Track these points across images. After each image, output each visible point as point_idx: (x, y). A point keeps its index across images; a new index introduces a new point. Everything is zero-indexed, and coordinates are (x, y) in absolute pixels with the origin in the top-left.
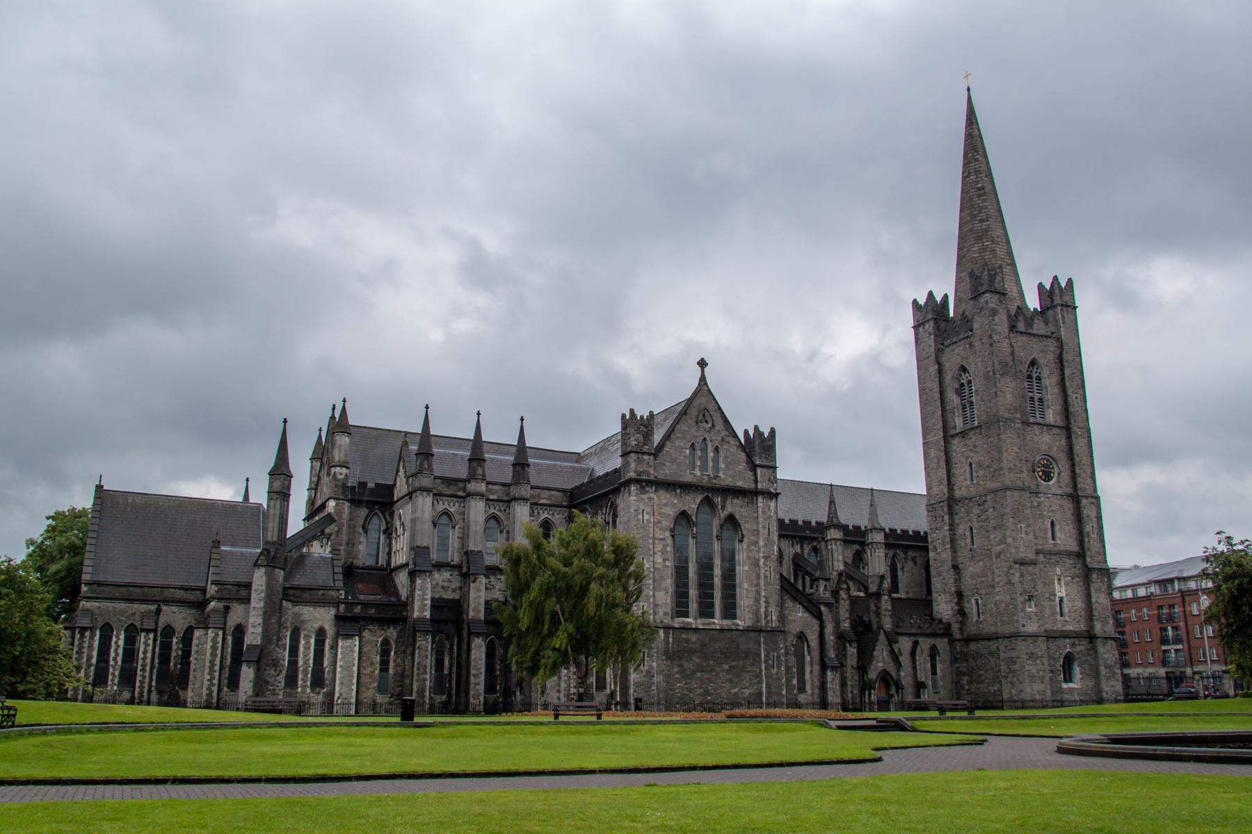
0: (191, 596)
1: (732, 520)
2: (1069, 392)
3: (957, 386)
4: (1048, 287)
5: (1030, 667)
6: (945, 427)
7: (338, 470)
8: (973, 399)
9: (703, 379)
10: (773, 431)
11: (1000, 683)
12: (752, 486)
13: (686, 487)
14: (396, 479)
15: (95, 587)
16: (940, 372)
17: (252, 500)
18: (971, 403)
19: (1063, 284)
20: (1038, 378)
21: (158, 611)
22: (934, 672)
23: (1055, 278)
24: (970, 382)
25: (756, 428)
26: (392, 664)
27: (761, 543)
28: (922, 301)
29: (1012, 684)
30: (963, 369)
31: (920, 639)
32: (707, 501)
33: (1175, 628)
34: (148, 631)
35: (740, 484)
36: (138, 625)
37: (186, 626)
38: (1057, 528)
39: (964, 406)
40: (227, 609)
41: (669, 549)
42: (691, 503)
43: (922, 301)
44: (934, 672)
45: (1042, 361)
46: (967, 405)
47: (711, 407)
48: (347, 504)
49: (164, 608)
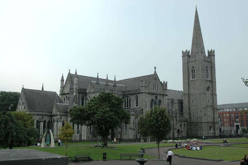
0: (49, 114)
1: (160, 100)
2: (213, 73)
3: (191, 70)
4: (210, 51)
5: (205, 129)
6: (188, 80)
7: (76, 86)
8: (195, 74)
9: (155, 71)
10: (167, 82)
11: (198, 131)
12: (163, 94)
13: (153, 94)
14: (87, 88)
15: (30, 112)
16: (188, 67)
17: (44, 90)
18: (194, 75)
19: (213, 50)
20: (208, 70)
21: (43, 117)
22: (184, 129)
23: (212, 50)
24: (194, 70)
25: (164, 81)
26: (92, 128)
27: (165, 105)
28: (184, 51)
29: (201, 131)
30: (193, 67)
31: (182, 122)
32: (156, 96)
33: (220, 119)
34: (42, 122)
35: (161, 93)
36: (39, 120)
37: (48, 120)
38: (209, 100)
39: (193, 75)
40: (61, 117)
41: (150, 106)
42: (154, 97)
43: (184, 51)
44: (184, 129)
45: (208, 67)
46: (194, 76)
47: (157, 77)
48: (78, 93)
49: (44, 116)
